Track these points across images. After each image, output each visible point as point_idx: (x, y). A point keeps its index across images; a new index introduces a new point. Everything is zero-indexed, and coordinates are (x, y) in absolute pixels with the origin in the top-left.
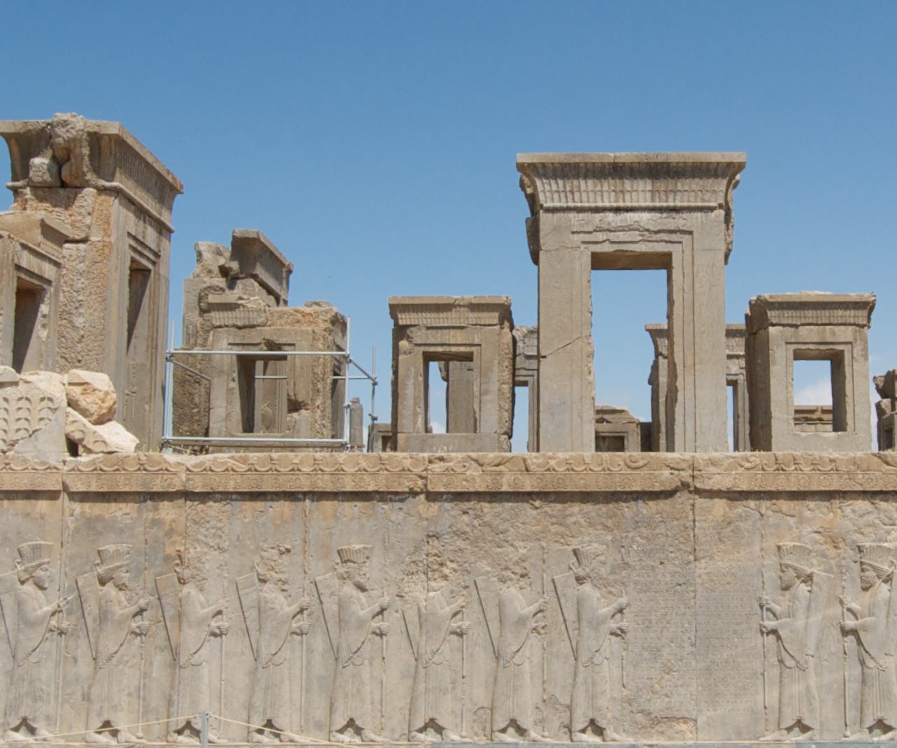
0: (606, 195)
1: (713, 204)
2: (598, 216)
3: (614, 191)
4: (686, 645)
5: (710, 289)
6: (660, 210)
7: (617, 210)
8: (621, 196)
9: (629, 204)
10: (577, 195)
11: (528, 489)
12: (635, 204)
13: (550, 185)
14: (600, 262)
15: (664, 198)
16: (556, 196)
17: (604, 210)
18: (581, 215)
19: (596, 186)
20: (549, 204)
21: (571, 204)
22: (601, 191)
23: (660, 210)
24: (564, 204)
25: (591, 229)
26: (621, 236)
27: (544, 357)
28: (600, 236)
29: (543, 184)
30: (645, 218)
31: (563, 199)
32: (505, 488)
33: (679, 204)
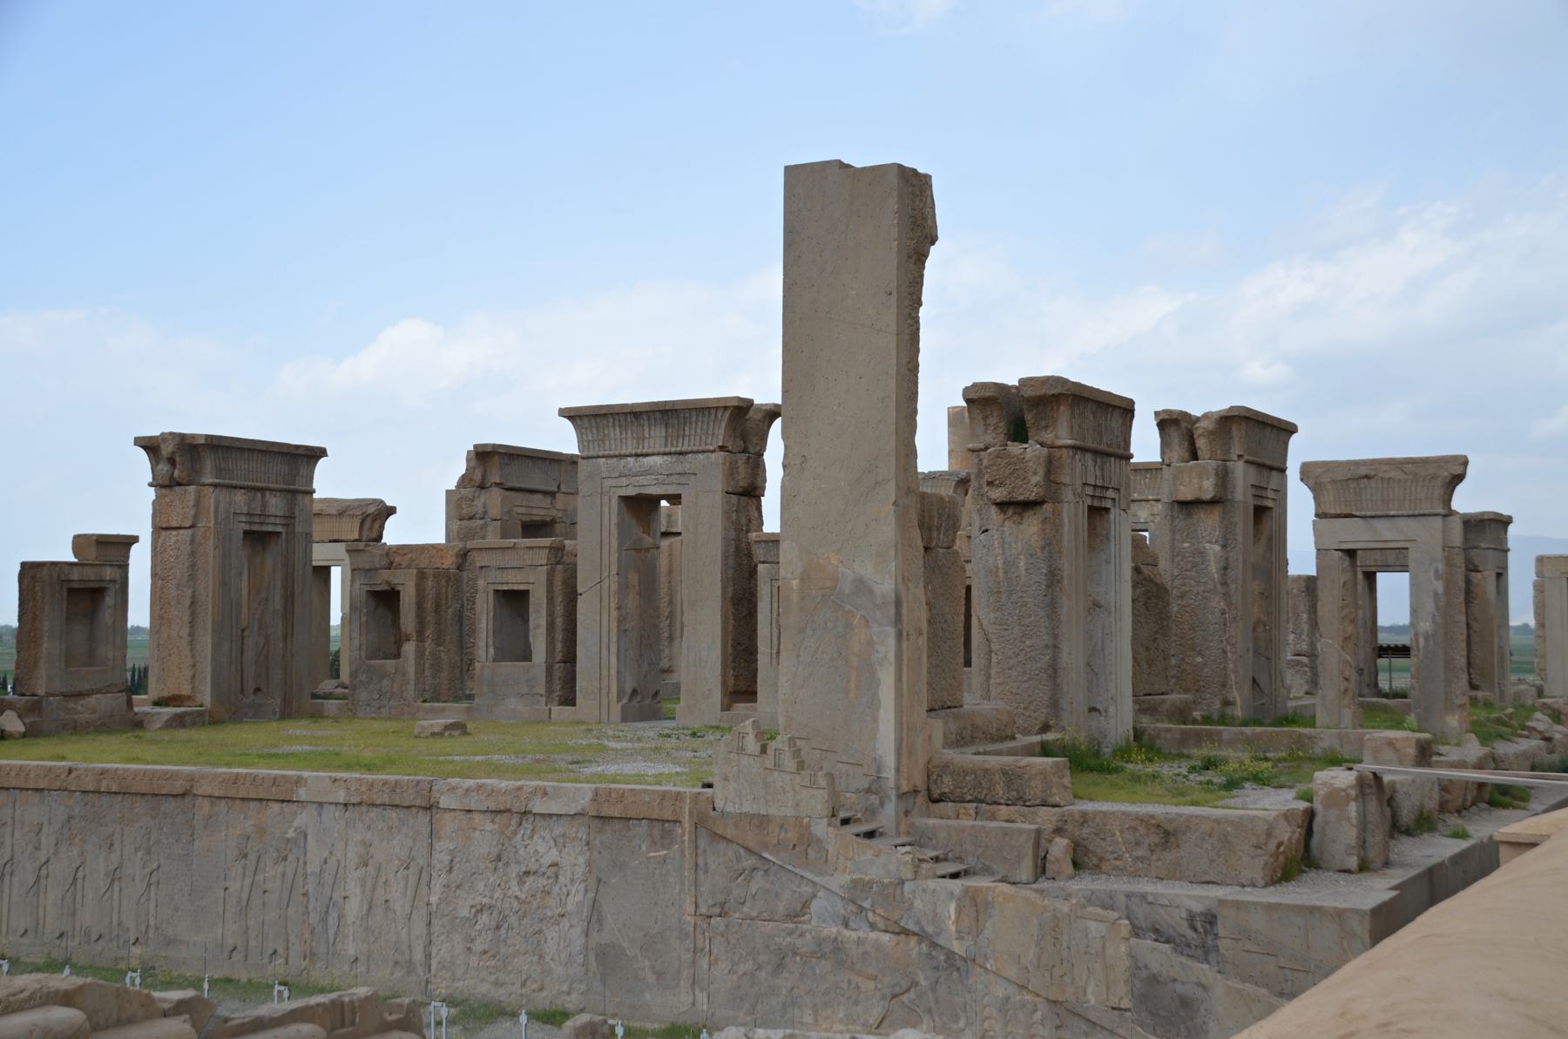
0: (630, 441)
1: (711, 448)
2: (623, 461)
4: (186, 894)
6: (670, 454)
7: (637, 455)
8: (641, 443)
9: (645, 451)
10: (607, 443)
11: (113, 790)
12: (650, 451)
15: (675, 442)
16: (591, 444)
18: (610, 461)
21: (601, 453)
22: (626, 439)
23: (670, 454)
24: (595, 454)
26: (641, 480)
27: (581, 594)
28: (624, 481)
30: (658, 463)
31: (597, 449)
32: (103, 790)
33: (686, 448)
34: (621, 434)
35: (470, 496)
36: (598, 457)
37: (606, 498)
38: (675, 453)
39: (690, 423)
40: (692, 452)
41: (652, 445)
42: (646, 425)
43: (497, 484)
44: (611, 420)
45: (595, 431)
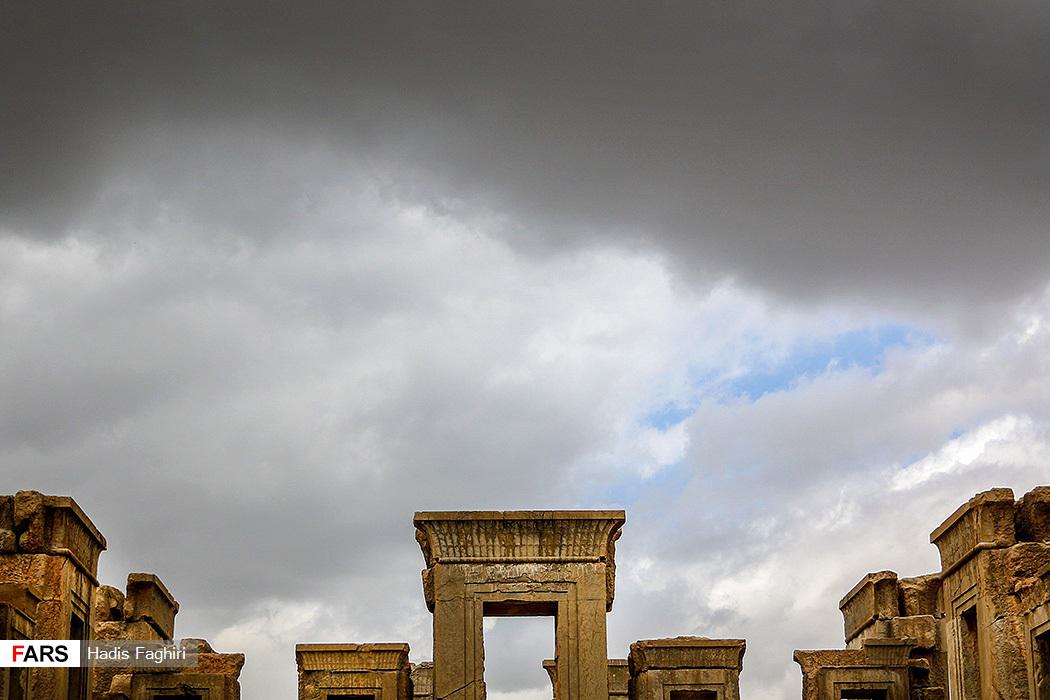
2: (490, 569)
3: (504, 545)
5: (593, 635)
7: (508, 562)
9: (517, 558)
12: (524, 558)
13: (445, 541)
14: (492, 609)
16: (451, 550)
17: (495, 562)
19: (487, 541)
20: (445, 558)
21: (465, 559)
22: (493, 546)
24: (458, 559)
25: (483, 580)
28: (492, 587)
29: (439, 539)
33: (563, 557)
34: (487, 541)
35: (116, 629)
36: (458, 563)
37: (471, 603)
38: (551, 562)
39: (569, 535)
40: (574, 561)
41: (524, 553)
42: (516, 531)
43: (148, 619)
44: (475, 527)
45: (455, 537)
